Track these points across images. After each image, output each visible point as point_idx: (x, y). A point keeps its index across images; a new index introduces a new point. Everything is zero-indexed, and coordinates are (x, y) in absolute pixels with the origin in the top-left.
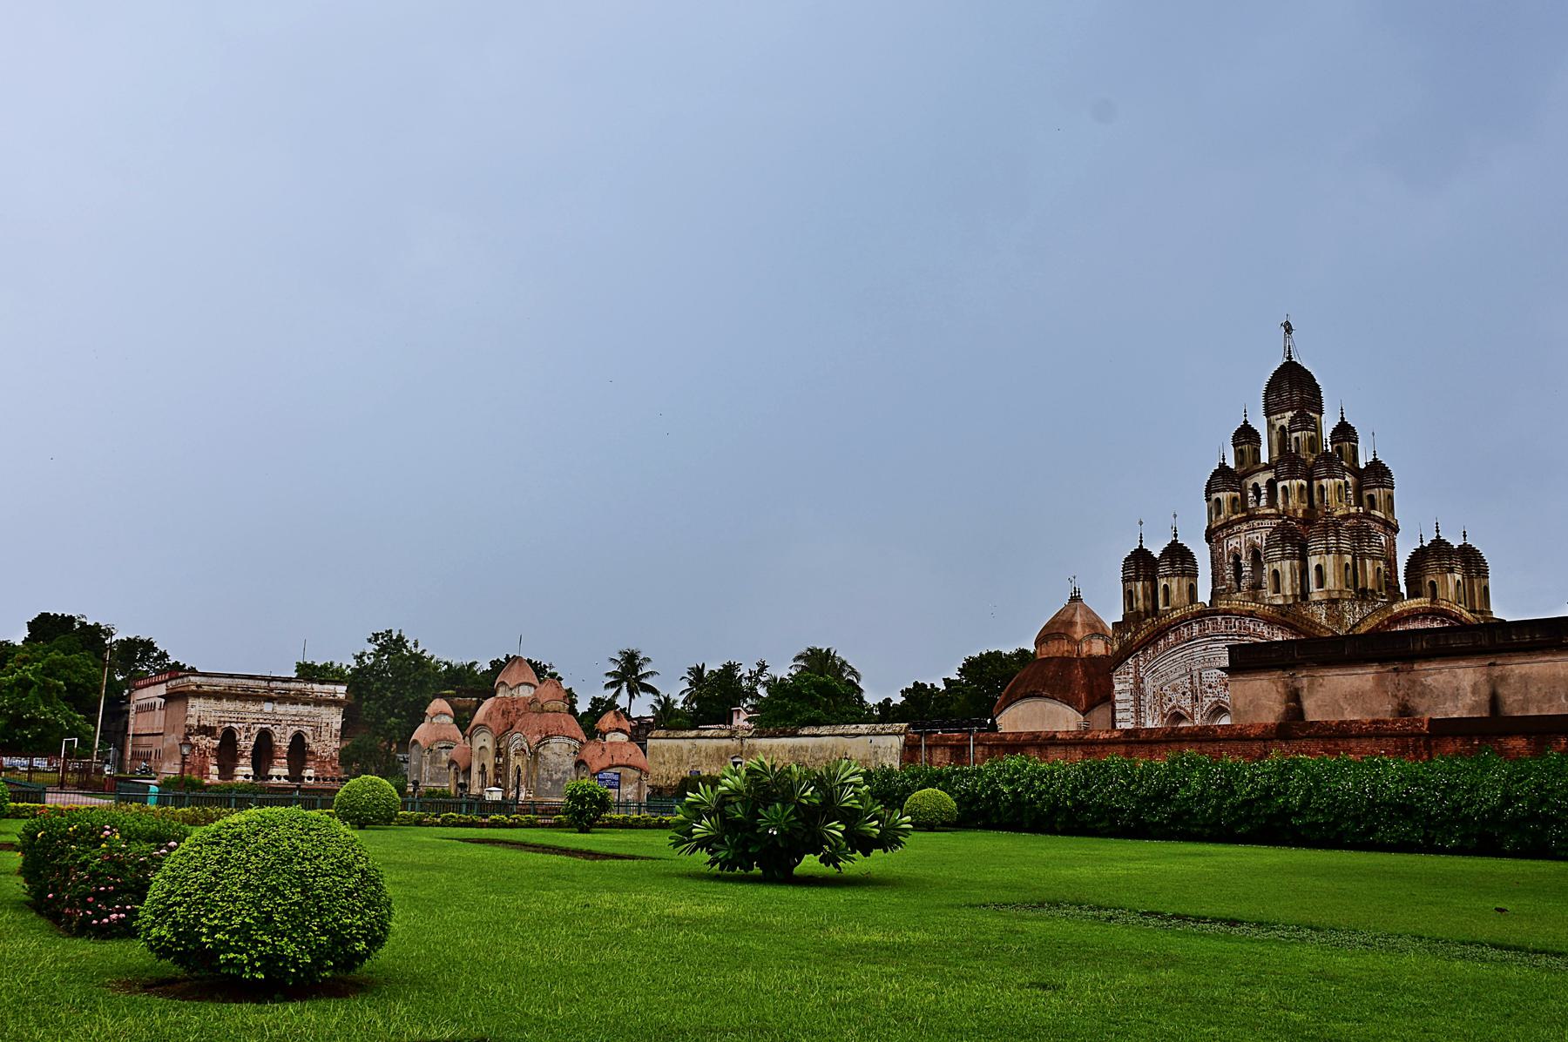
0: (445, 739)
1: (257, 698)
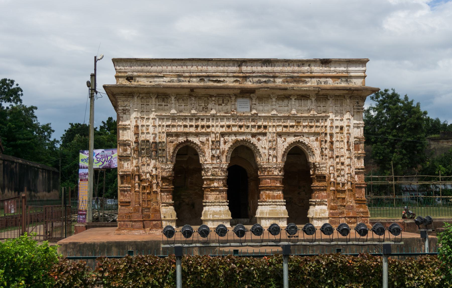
1: (223, 96)
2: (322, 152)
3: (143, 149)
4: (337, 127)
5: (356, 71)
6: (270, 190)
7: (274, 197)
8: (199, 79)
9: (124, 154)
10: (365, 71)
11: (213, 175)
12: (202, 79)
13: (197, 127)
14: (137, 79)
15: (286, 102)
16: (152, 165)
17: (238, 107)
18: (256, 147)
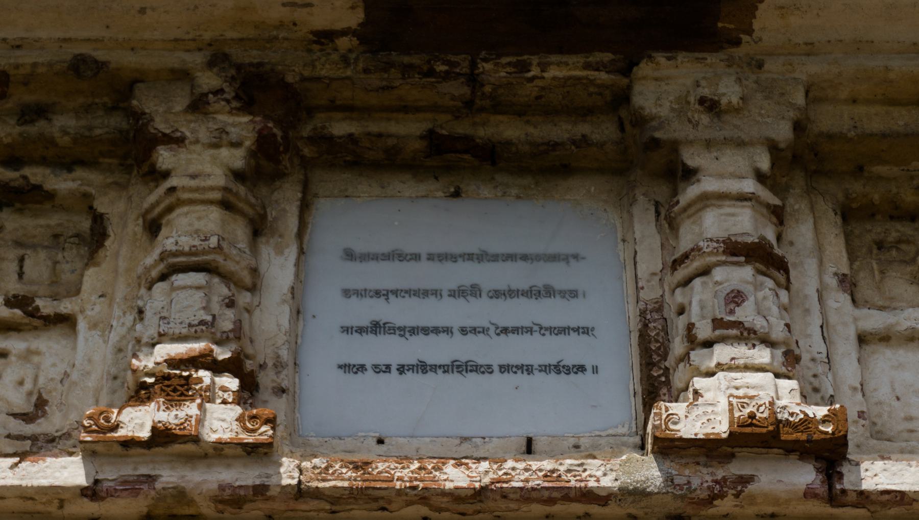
17: (324, 351)
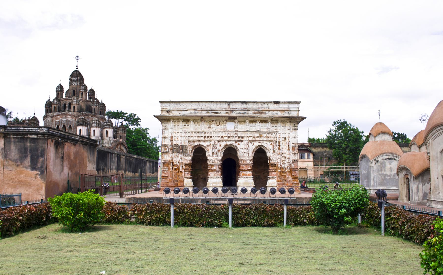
0: (389, 153)
1: (219, 120)
2: (274, 151)
3: (175, 149)
4: (282, 137)
5: (293, 108)
6: (245, 171)
7: (246, 175)
8: (206, 112)
9: (165, 151)
10: (299, 108)
11: (213, 163)
12: (208, 111)
13: (205, 137)
14: (173, 112)
15: (254, 124)
16: (179, 157)
18: (237, 148)
